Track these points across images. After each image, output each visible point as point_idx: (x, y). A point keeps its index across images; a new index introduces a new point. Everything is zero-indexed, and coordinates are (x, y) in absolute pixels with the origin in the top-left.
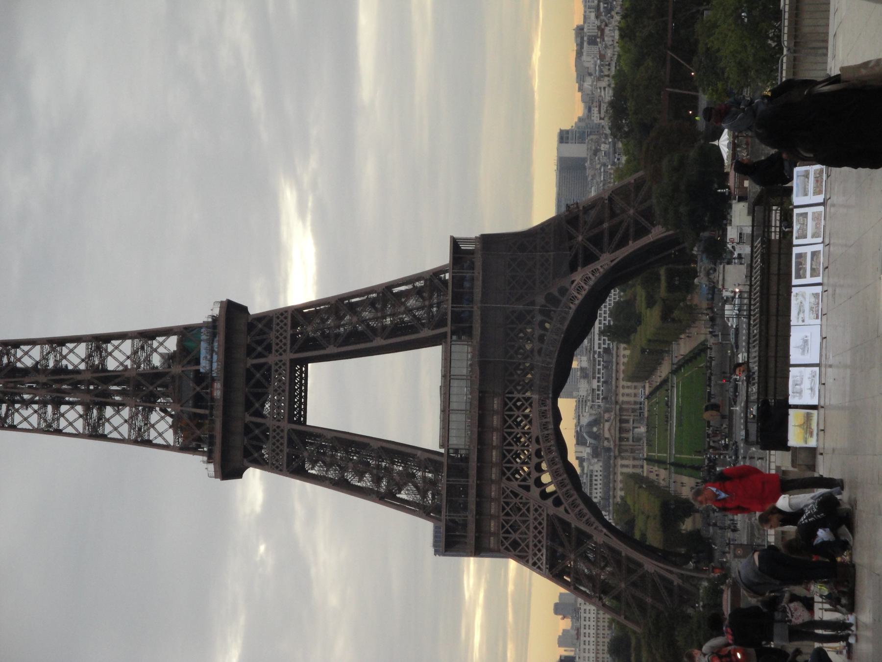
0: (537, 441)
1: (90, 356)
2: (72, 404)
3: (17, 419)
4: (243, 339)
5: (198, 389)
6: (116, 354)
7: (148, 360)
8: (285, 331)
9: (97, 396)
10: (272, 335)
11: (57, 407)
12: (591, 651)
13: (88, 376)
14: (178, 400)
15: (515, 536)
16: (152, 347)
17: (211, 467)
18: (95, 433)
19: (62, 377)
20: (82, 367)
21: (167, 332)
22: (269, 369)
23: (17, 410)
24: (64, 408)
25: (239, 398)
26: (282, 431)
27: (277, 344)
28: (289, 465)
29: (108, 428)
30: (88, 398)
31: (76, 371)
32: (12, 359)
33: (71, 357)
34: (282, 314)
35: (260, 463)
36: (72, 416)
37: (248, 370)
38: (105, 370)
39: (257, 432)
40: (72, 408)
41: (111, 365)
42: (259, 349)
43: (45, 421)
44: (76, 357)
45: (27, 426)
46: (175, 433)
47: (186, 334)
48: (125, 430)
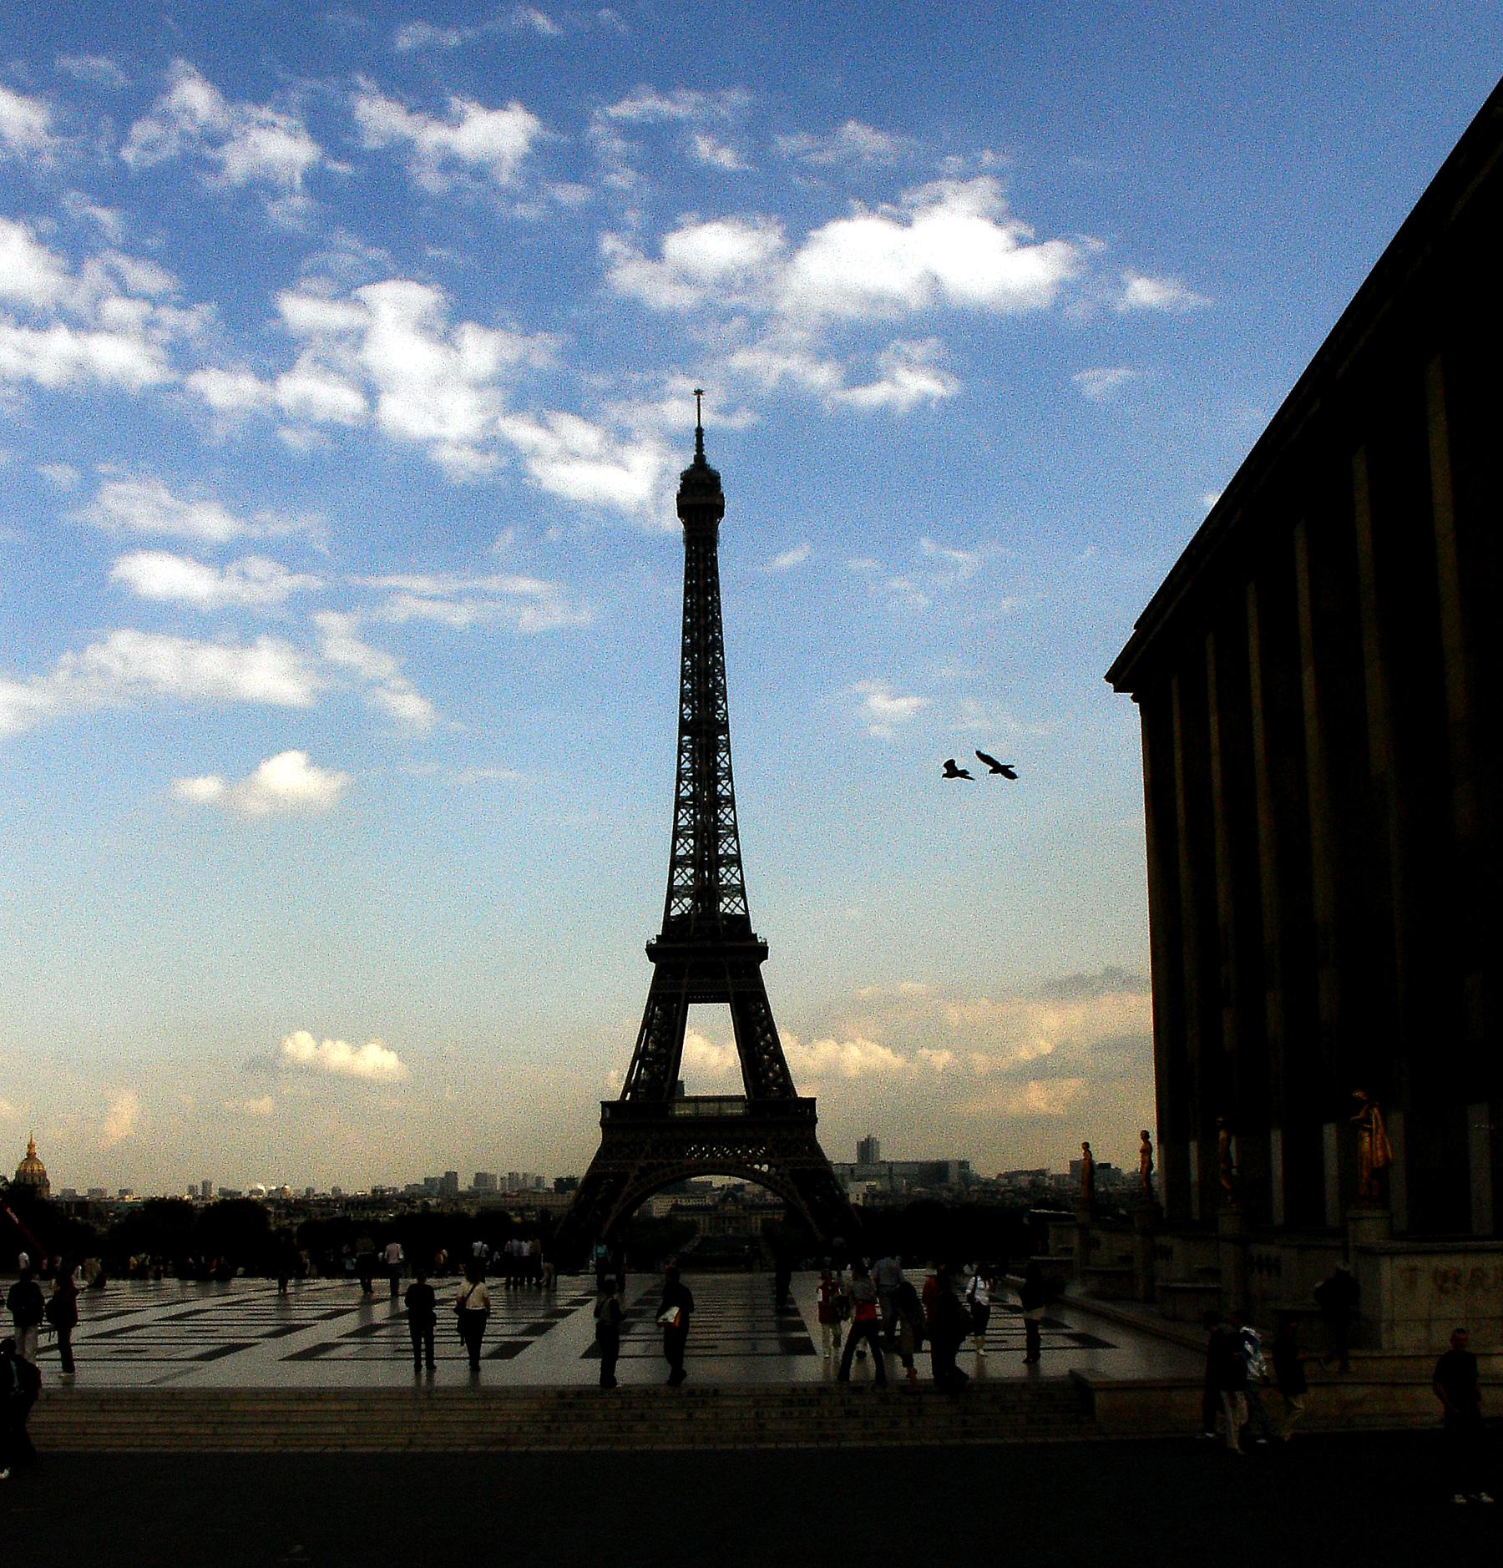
6: (729, 876)
11: (690, 836)
14: (699, 917)
18: (676, 862)
20: (721, 852)
24: (691, 842)
33: (725, 846)
36: (686, 847)
41: (723, 870)
47: (744, 920)
48: (678, 882)
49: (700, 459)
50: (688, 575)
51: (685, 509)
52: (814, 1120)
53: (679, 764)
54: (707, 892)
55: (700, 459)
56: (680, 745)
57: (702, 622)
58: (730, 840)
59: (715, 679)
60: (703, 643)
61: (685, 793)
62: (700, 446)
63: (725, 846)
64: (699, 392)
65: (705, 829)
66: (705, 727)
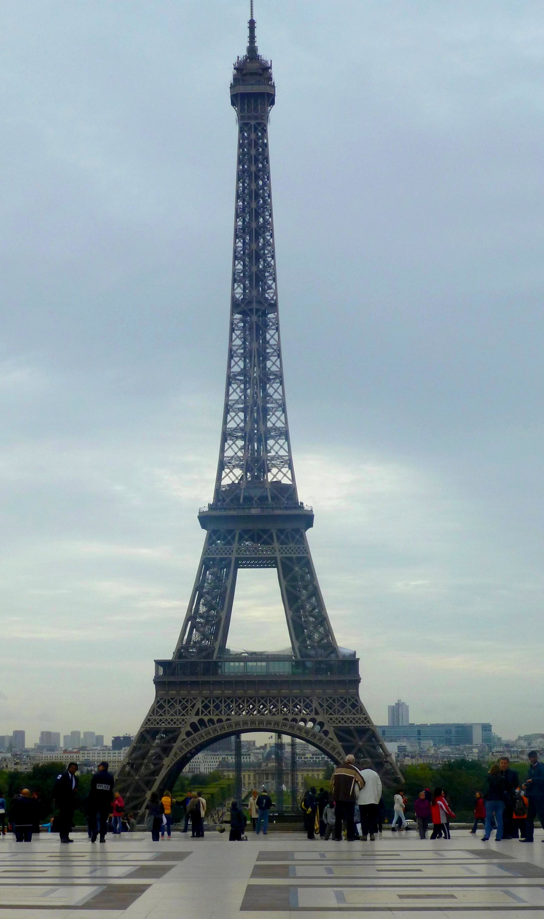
0: (228, 720)
1: (275, 429)
2: (245, 420)
3: (235, 386)
4: (288, 526)
5: (256, 499)
6: (277, 447)
7: (274, 466)
8: (295, 553)
9: (250, 435)
10: (292, 545)
11: (244, 410)
12: (93, 758)
13: (262, 429)
15: (167, 707)
16: (282, 467)
17: (206, 509)
18: (226, 435)
19: (261, 415)
20: (269, 425)
21: (293, 479)
22: (271, 545)
23: (239, 387)
24: (242, 415)
26: (230, 554)
27: (286, 548)
28: (210, 559)
30: (248, 429)
31: (265, 420)
32: (272, 381)
34: (306, 550)
35: (210, 541)
36: (236, 420)
37: (268, 530)
38: (267, 439)
39: (229, 538)
40: (242, 420)
41: (271, 442)
42: (282, 537)
43: (234, 404)
44: (274, 420)
45: (230, 392)
46: (228, 485)
48: (229, 453)
49: (252, 50)
50: (240, 161)
51: (238, 99)
52: (357, 681)
53: (231, 340)
54: (256, 465)
55: (252, 50)
56: (232, 323)
57: (254, 205)
58: (278, 414)
59: (265, 261)
60: (254, 225)
61: (236, 369)
62: (252, 38)
63: (273, 419)
65: (255, 403)
66: (254, 306)
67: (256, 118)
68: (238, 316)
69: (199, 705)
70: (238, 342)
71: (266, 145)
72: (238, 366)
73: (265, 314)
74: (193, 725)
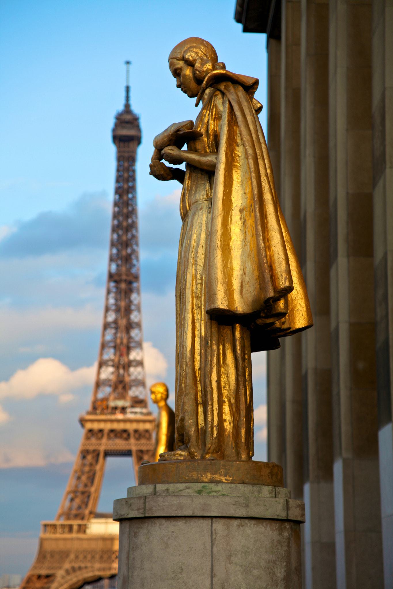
1: (135, 361)
11: (115, 347)
25: (116, 426)
29: (103, 369)
31: (128, 354)
49: (127, 106)
50: (117, 181)
53: (107, 299)
55: (127, 106)
60: (125, 224)
62: (127, 98)
64: (128, 63)
65: (122, 343)
67: (128, 152)
68: (112, 284)
69: (72, 556)
70: (112, 301)
71: (134, 171)
72: (112, 317)
73: (130, 283)
74: (67, 572)
